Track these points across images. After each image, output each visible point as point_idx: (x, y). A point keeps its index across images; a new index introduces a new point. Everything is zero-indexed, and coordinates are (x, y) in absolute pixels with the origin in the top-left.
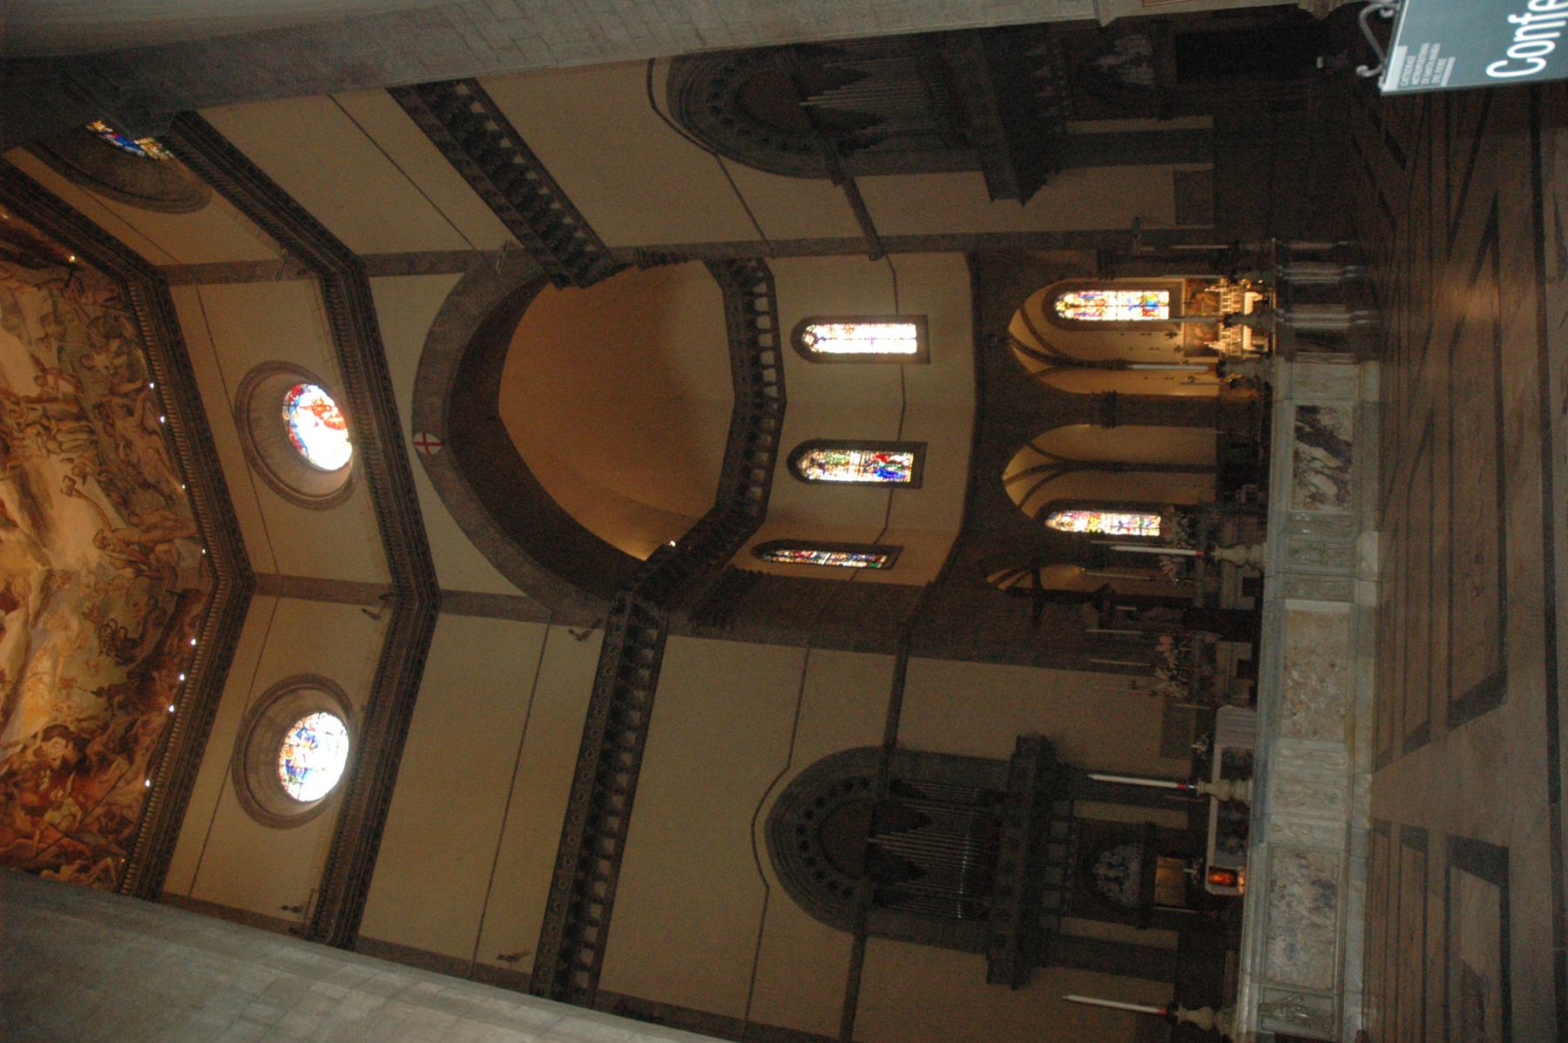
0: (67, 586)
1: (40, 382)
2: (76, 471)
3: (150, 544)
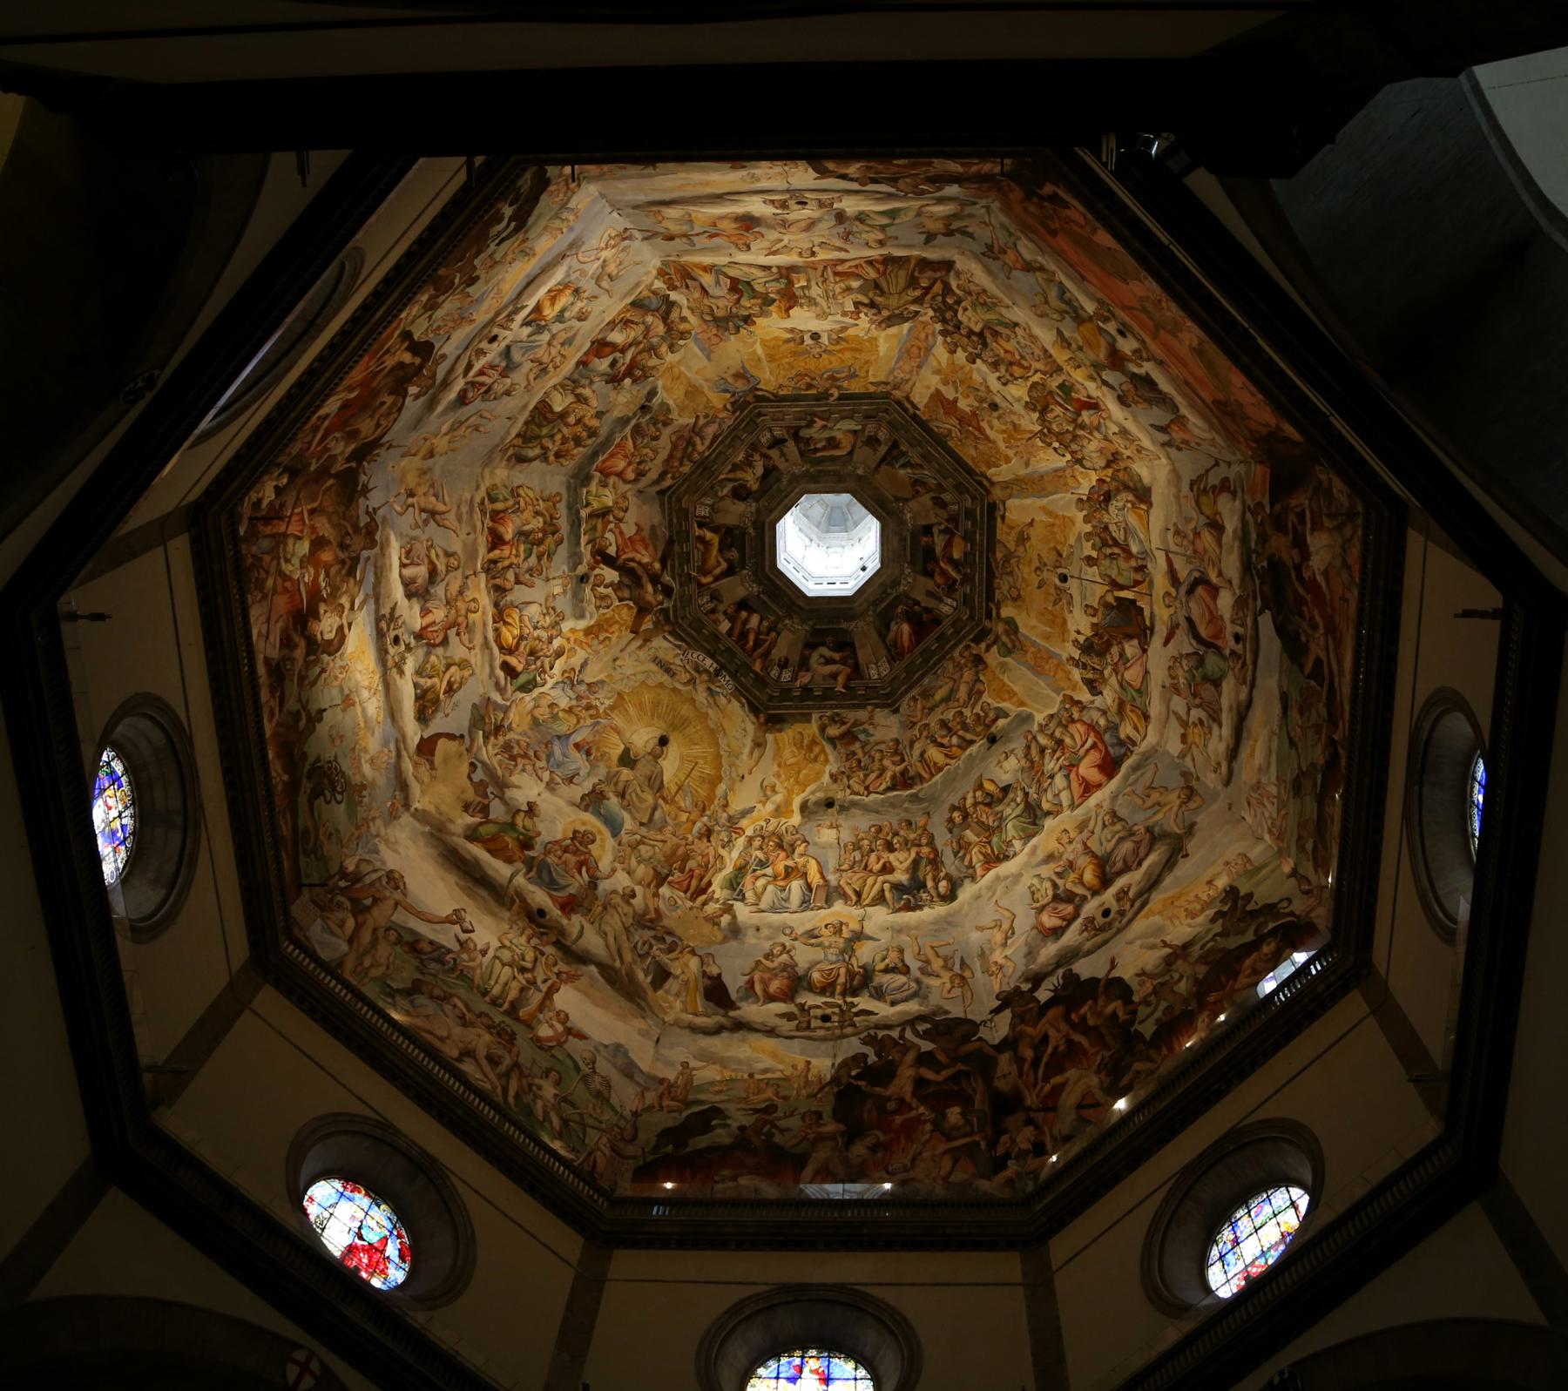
0: (389, 804)
1: (562, 1016)
2: (472, 946)
3: (360, 918)
